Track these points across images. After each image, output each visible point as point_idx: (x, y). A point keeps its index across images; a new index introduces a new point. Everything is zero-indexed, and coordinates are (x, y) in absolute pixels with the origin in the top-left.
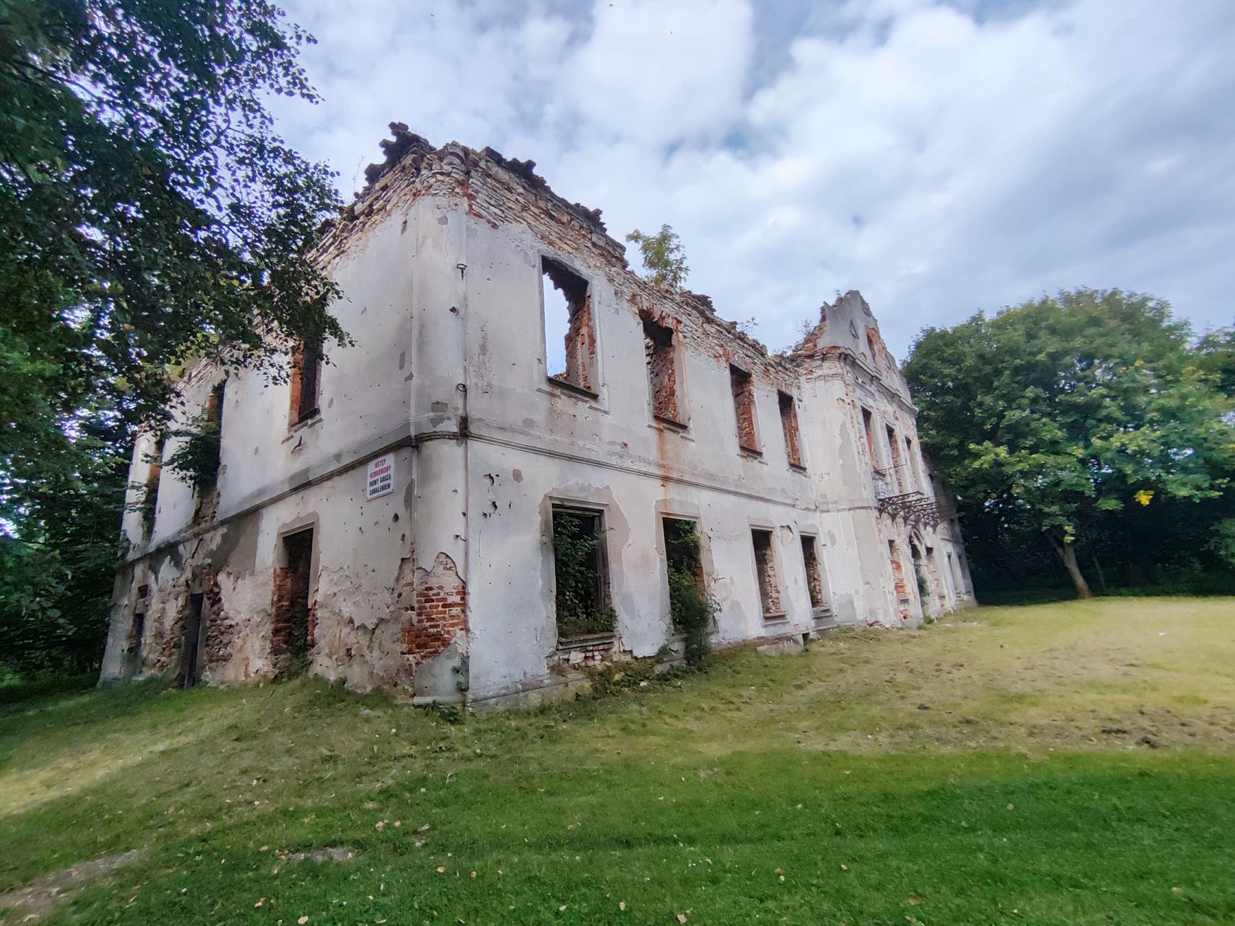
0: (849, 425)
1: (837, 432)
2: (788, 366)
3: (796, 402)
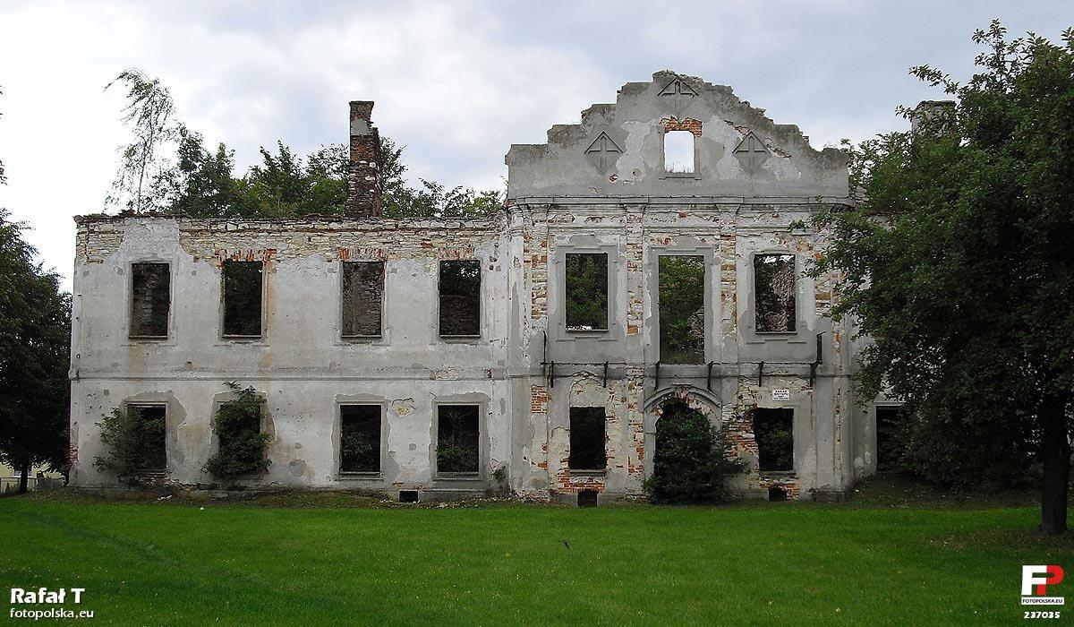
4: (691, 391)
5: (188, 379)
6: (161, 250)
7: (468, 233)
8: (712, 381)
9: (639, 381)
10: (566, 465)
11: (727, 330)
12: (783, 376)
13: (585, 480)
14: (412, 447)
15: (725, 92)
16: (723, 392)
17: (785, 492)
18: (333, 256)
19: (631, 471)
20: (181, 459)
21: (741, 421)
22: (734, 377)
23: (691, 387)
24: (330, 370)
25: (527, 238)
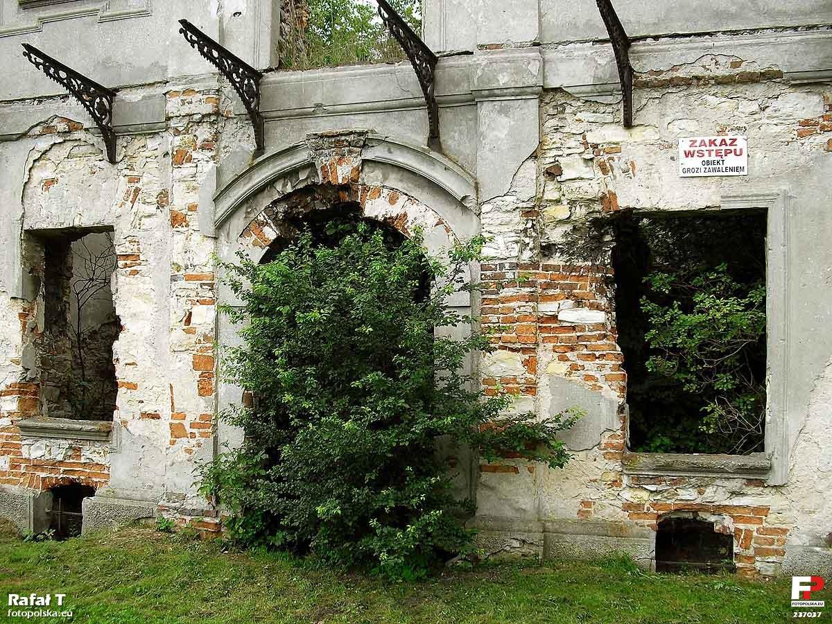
4: (369, 155)
8: (446, 116)
9: (204, 133)
10: (11, 404)
12: (721, 82)
13: (58, 450)
16: (485, 152)
17: (726, 540)
21: (557, 260)
22: (520, 93)
23: (364, 140)
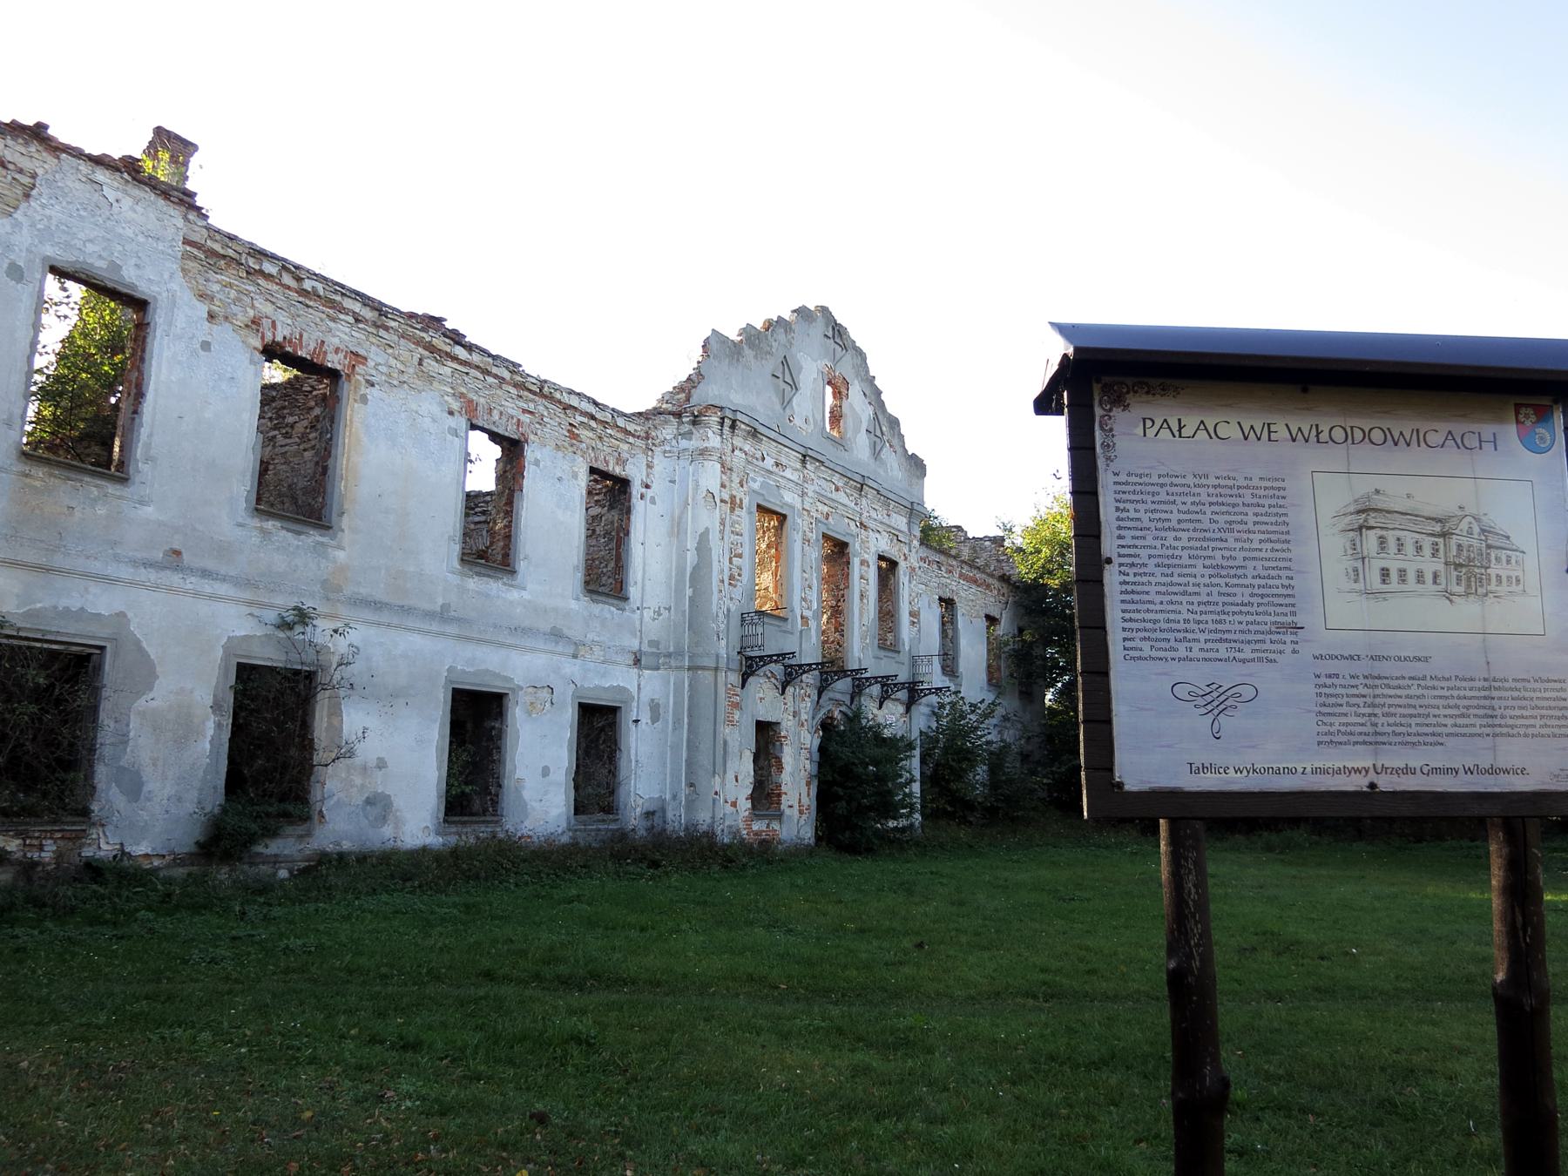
0: (714, 537)
1: (691, 544)
2: (631, 427)
3: (636, 489)
5: (170, 589)
6: (133, 261)
7: (619, 435)
11: (863, 638)
14: (546, 772)
15: (861, 354)
18: (455, 406)
19: (801, 812)
20: (134, 787)
24: (443, 615)
25: (726, 469)
